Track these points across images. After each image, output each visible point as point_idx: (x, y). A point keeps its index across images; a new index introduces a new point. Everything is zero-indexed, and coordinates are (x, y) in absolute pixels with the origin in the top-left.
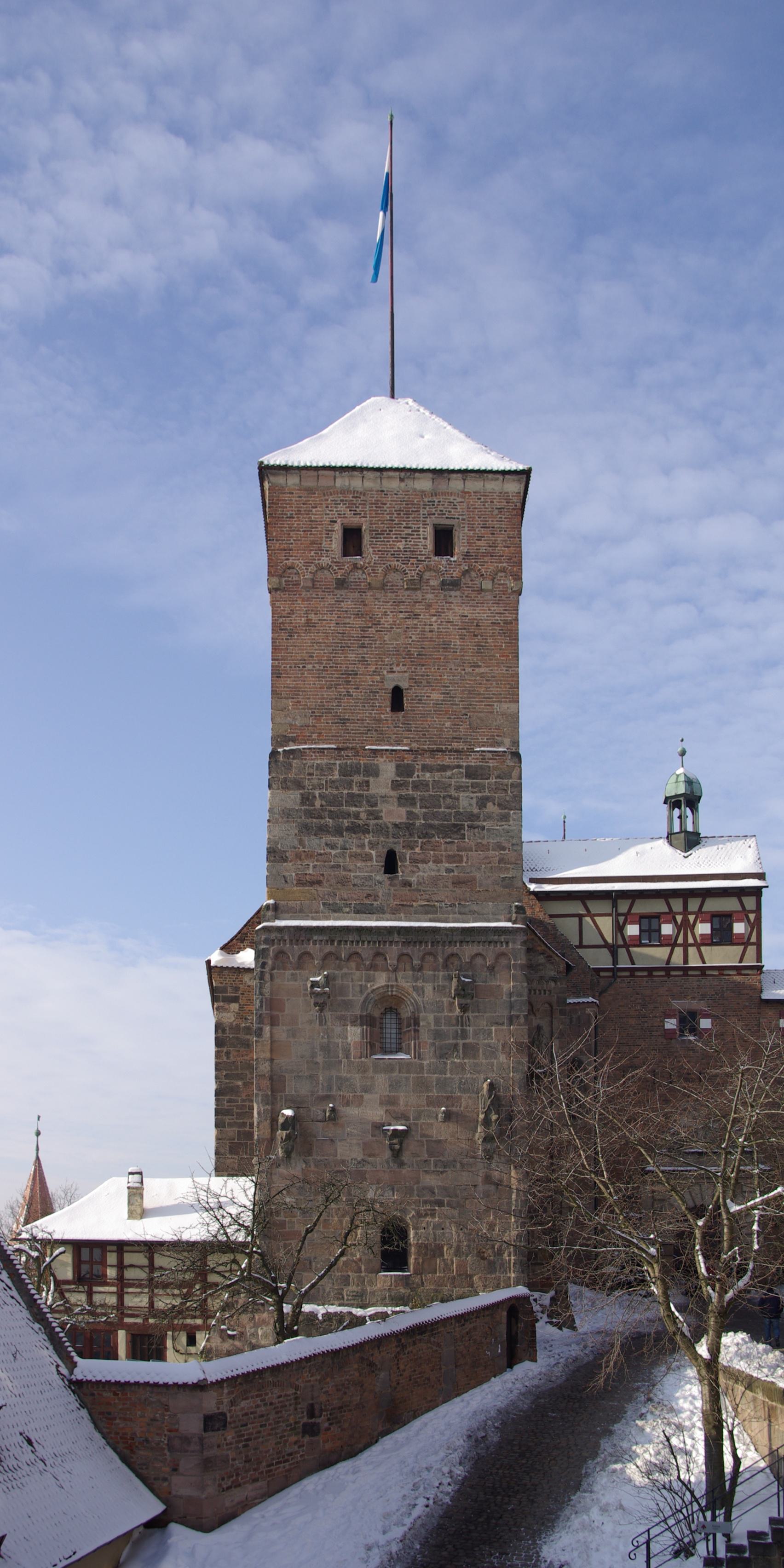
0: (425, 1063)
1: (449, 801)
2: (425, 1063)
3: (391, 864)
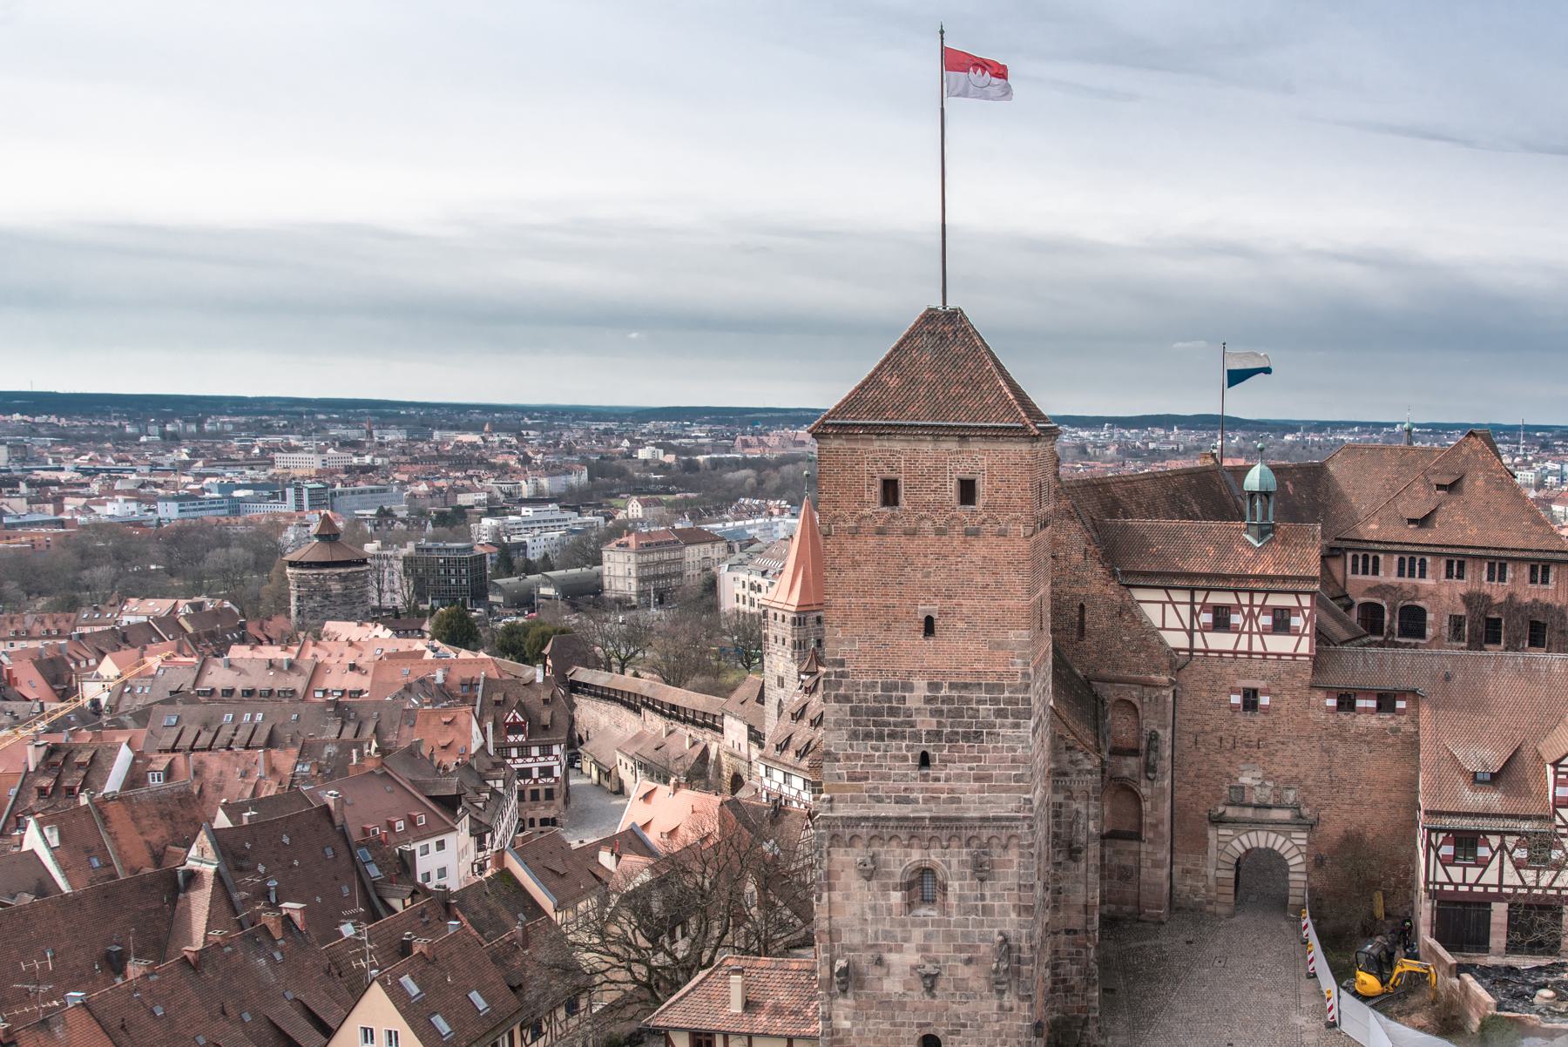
0: (952, 919)
1: (971, 712)
2: (952, 919)
3: (925, 760)
